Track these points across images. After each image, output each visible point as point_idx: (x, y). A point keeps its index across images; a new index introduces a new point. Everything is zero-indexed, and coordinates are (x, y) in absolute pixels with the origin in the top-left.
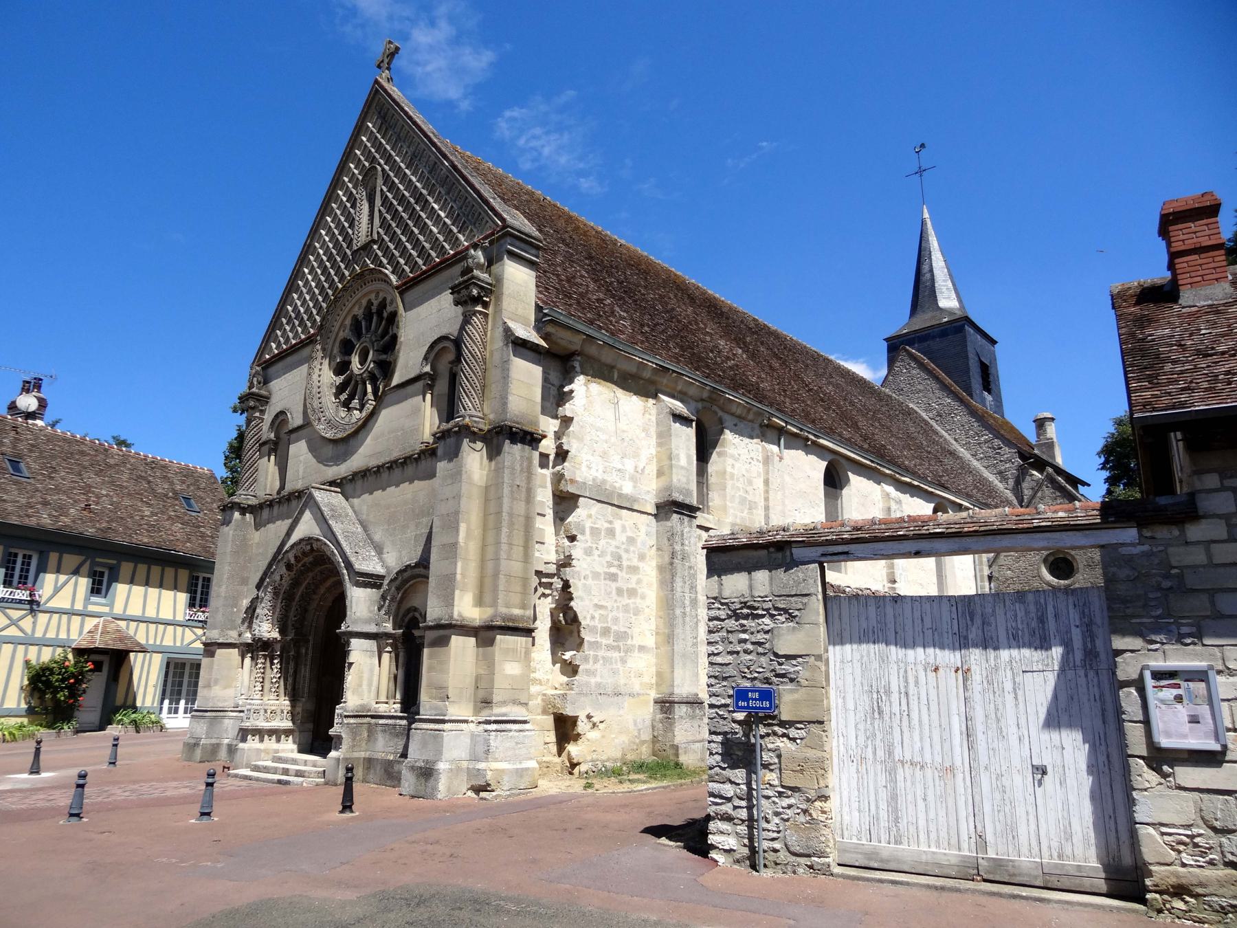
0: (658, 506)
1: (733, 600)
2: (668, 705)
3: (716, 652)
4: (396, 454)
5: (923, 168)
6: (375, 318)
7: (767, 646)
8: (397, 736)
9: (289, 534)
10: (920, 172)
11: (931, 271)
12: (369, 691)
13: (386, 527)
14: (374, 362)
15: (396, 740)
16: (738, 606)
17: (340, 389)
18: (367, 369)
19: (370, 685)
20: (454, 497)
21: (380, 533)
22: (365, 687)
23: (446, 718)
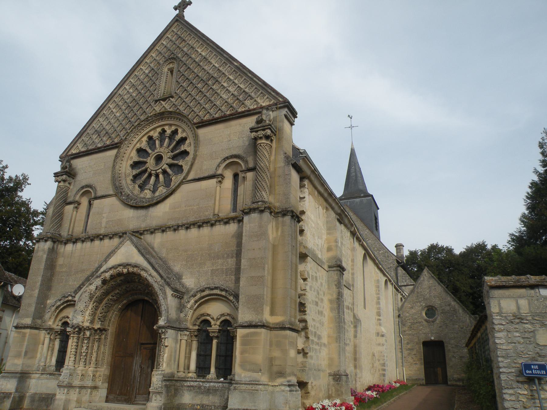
0: (329, 267)
1: (509, 315)
2: (338, 376)
3: (502, 343)
4: (192, 219)
5: (353, 126)
6: (167, 140)
7: (532, 339)
8: (202, 393)
9: (106, 260)
10: (351, 127)
11: (355, 172)
12: (174, 365)
13: (184, 263)
14: (167, 164)
15: (201, 396)
16: (512, 318)
17: (135, 177)
18: (161, 168)
19: (175, 361)
20: (260, 249)
21: (179, 266)
22: (173, 362)
23: (259, 383)
